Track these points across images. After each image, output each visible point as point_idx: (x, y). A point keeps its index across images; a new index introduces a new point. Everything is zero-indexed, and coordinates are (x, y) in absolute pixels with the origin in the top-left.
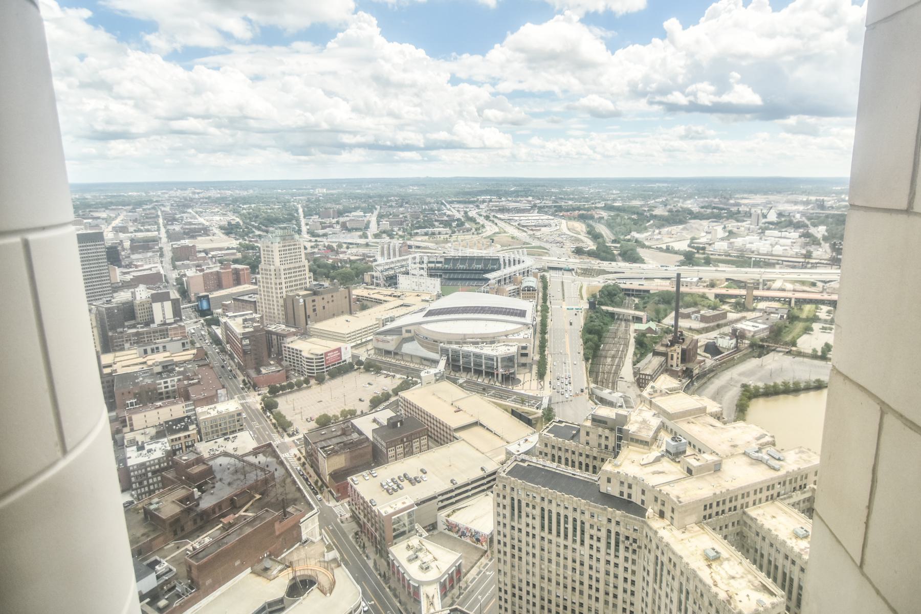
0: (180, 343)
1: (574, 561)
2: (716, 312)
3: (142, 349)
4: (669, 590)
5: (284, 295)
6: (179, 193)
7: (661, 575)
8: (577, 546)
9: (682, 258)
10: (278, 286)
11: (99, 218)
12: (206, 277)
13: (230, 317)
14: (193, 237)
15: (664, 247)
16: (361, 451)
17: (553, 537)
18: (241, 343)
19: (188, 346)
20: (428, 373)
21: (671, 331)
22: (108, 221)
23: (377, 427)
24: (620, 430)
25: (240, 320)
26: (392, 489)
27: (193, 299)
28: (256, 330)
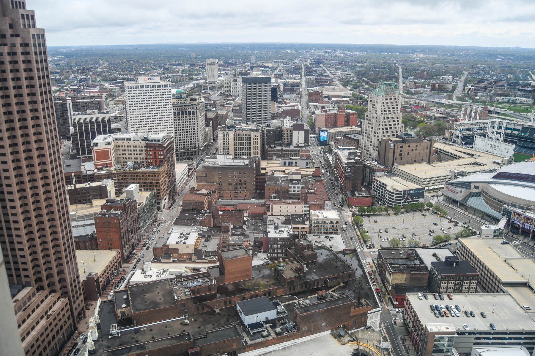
0: (305, 162)
3: (283, 161)
5: (380, 138)
6: (316, 52)
10: (377, 131)
11: (267, 67)
12: (328, 116)
13: (340, 149)
14: (322, 86)
16: (420, 276)
18: (345, 170)
19: (311, 165)
20: (488, 228)
23: (436, 261)
25: (346, 153)
27: (317, 131)
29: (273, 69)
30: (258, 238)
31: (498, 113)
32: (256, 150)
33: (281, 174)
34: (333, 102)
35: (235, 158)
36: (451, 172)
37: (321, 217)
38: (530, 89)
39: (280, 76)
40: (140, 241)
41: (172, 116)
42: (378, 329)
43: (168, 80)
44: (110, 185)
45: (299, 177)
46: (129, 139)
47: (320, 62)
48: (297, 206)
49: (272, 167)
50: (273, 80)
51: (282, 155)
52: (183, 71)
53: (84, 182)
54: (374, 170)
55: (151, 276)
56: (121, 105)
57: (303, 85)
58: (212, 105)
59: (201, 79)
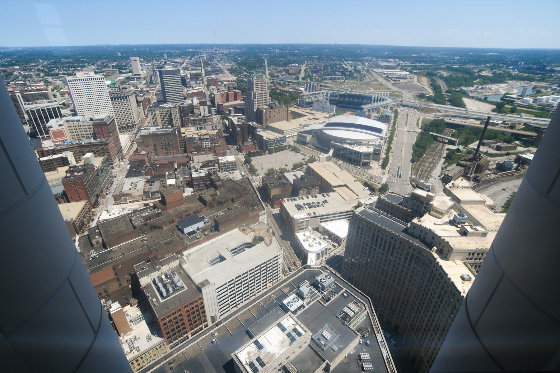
1: (386, 261)
2: (509, 145)
4: (435, 288)
6: (210, 50)
7: (433, 280)
8: (389, 255)
9: (494, 107)
12: (222, 95)
14: (216, 74)
15: (483, 98)
17: (377, 248)
21: (472, 152)
22: (181, 64)
23: (295, 178)
24: (428, 204)
25: (236, 118)
26: (299, 207)
28: (243, 123)
29: (181, 64)
30: (185, 178)
31: (325, 86)
32: (177, 121)
33: (196, 136)
34: (225, 85)
35: (163, 128)
36: (300, 125)
37: (225, 160)
38: (343, 70)
39: (186, 69)
40: (102, 192)
41: (110, 101)
42: (266, 223)
43: (102, 74)
44: (70, 156)
45: (208, 137)
46: (78, 121)
47: (213, 57)
48: (209, 155)
49: (189, 132)
50: (182, 71)
51: (194, 123)
52: (113, 66)
53: (47, 155)
54: (255, 128)
55: (114, 214)
56: (67, 95)
57: (204, 75)
58: (139, 91)
59: (129, 72)
